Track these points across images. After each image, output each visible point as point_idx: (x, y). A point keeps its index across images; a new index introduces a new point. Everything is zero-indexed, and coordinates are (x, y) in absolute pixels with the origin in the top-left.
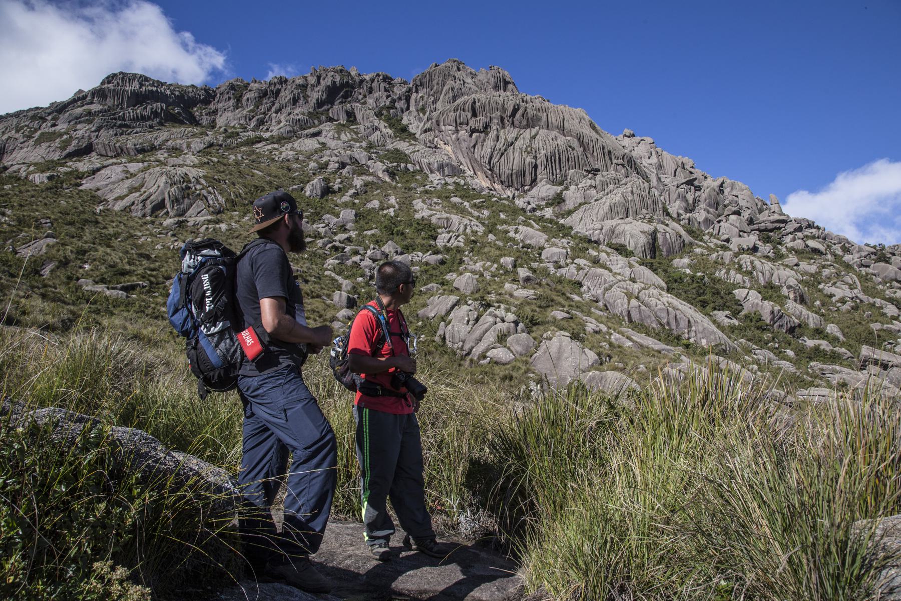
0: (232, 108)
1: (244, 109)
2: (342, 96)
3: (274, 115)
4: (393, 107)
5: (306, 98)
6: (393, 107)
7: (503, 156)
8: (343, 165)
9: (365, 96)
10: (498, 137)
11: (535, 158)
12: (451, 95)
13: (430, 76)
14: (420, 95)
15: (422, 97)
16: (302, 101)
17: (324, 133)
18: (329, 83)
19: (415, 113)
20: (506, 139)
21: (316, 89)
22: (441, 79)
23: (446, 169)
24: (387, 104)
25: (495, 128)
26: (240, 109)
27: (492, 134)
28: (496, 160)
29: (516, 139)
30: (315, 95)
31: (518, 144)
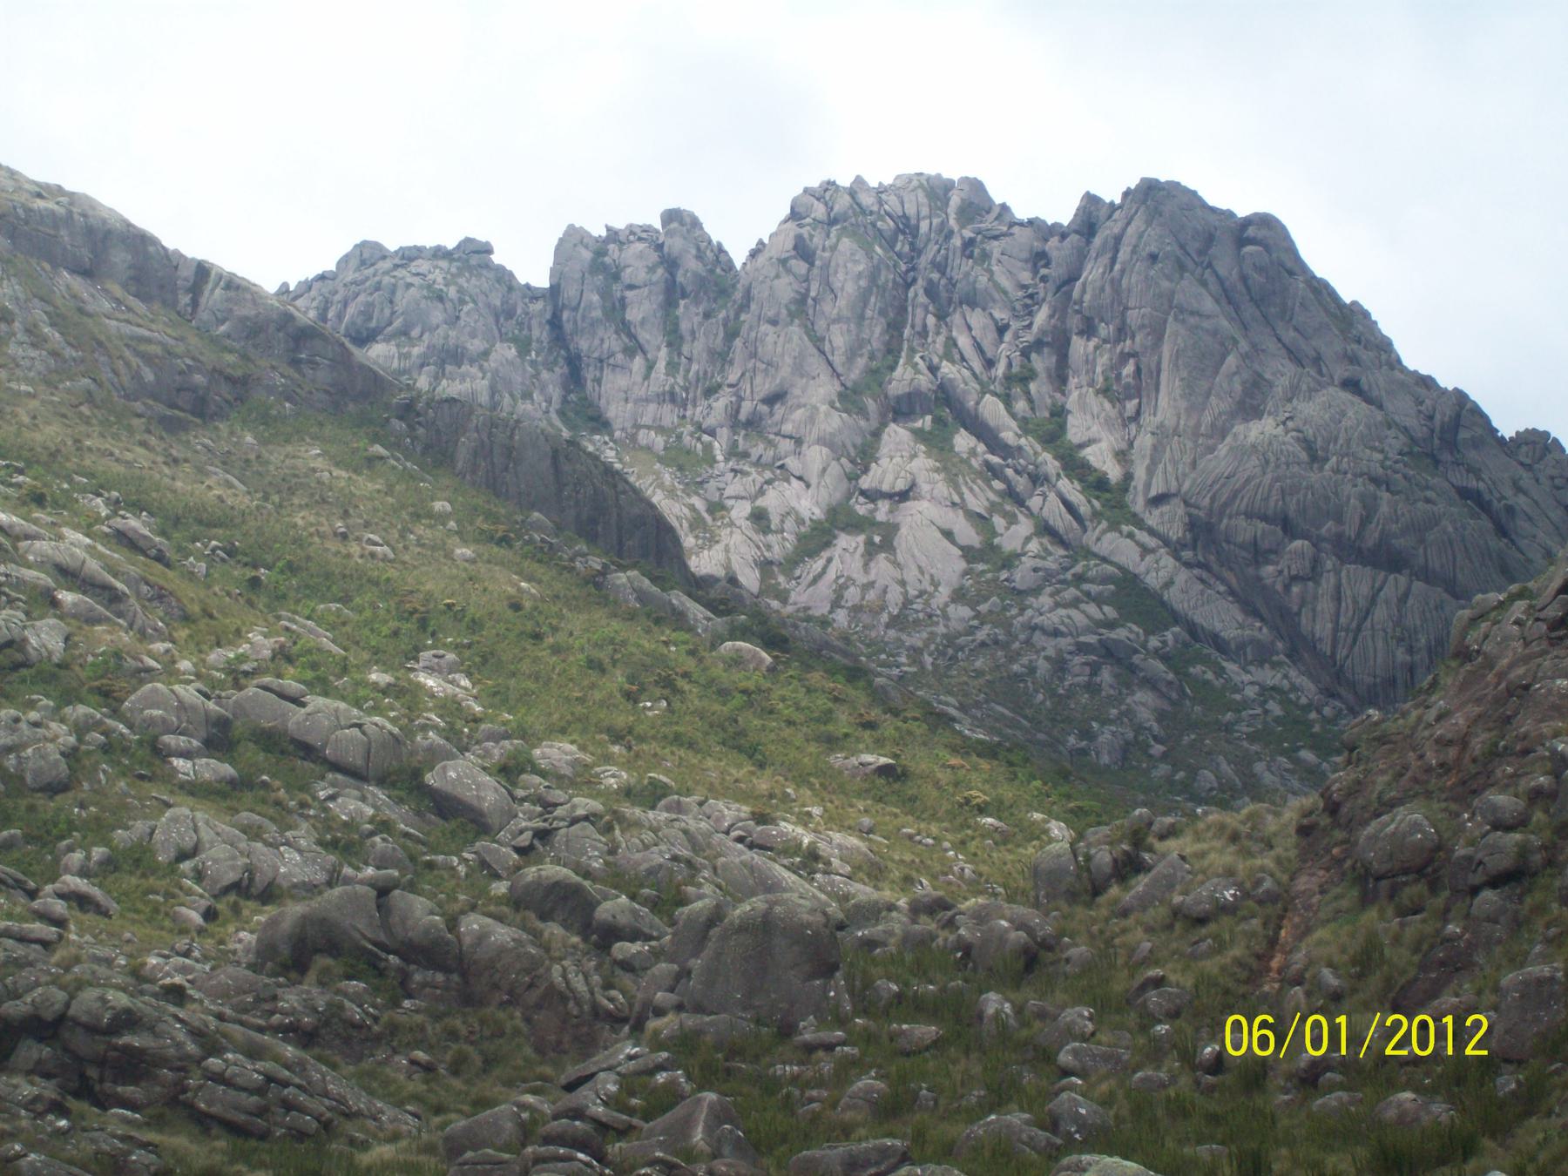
0: (620, 356)
1: (650, 367)
3: (764, 409)
7: (1356, 649)
8: (1095, 669)
10: (1338, 587)
11: (1411, 650)
17: (925, 487)
20: (1355, 602)
23: (1249, 650)
25: (1329, 564)
26: (638, 363)
27: (1328, 582)
28: (1345, 652)
29: (1373, 601)
31: (1380, 613)
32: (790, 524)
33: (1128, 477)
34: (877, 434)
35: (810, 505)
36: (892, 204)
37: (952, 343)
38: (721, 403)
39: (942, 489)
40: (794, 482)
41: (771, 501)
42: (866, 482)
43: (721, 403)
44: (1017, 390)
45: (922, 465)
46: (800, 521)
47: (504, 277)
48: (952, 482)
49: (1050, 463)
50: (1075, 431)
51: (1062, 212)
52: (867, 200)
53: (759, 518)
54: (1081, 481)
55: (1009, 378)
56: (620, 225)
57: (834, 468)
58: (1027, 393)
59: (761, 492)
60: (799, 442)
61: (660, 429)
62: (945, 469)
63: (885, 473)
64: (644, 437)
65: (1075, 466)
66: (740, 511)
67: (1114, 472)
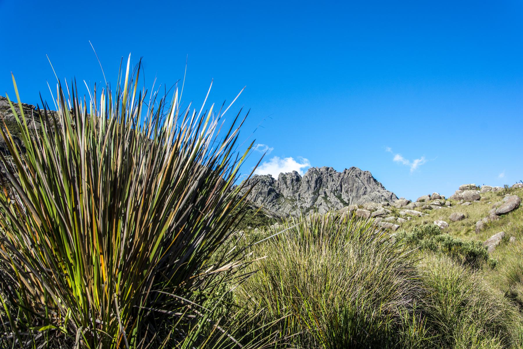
1: (290, 189)
2: (319, 183)
3: (303, 194)
4: (337, 190)
5: (310, 186)
6: (337, 190)
9: (326, 183)
12: (356, 190)
13: (348, 180)
14: (345, 186)
15: (346, 187)
16: (310, 188)
17: (323, 204)
18: (315, 179)
19: (345, 193)
21: (312, 182)
22: (352, 182)
24: (335, 189)
30: (313, 185)
32: (305, 208)
33: (349, 203)
34: (318, 197)
35: (308, 206)
36: (321, 170)
37: (327, 186)
38: (298, 193)
39: (325, 204)
40: (307, 203)
41: (303, 205)
42: (315, 203)
43: (298, 193)
44: (335, 192)
45: (323, 201)
46: (306, 208)
47: (273, 179)
48: (326, 203)
49: (339, 201)
50: (343, 197)
51: (342, 171)
52: (318, 170)
53: (302, 207)
54: (343, 203)
55: (334, 191)
56: (287, 172)
57: (311, 202)
58: (337, 192)
59: (302, 204)
60: (307, 198)
61: (290, 197)
62: (326, 202)
63: (318, 202)
64: (288, 198)
65: (342, 201)
66: (299, 206)
67: (347, 202)
